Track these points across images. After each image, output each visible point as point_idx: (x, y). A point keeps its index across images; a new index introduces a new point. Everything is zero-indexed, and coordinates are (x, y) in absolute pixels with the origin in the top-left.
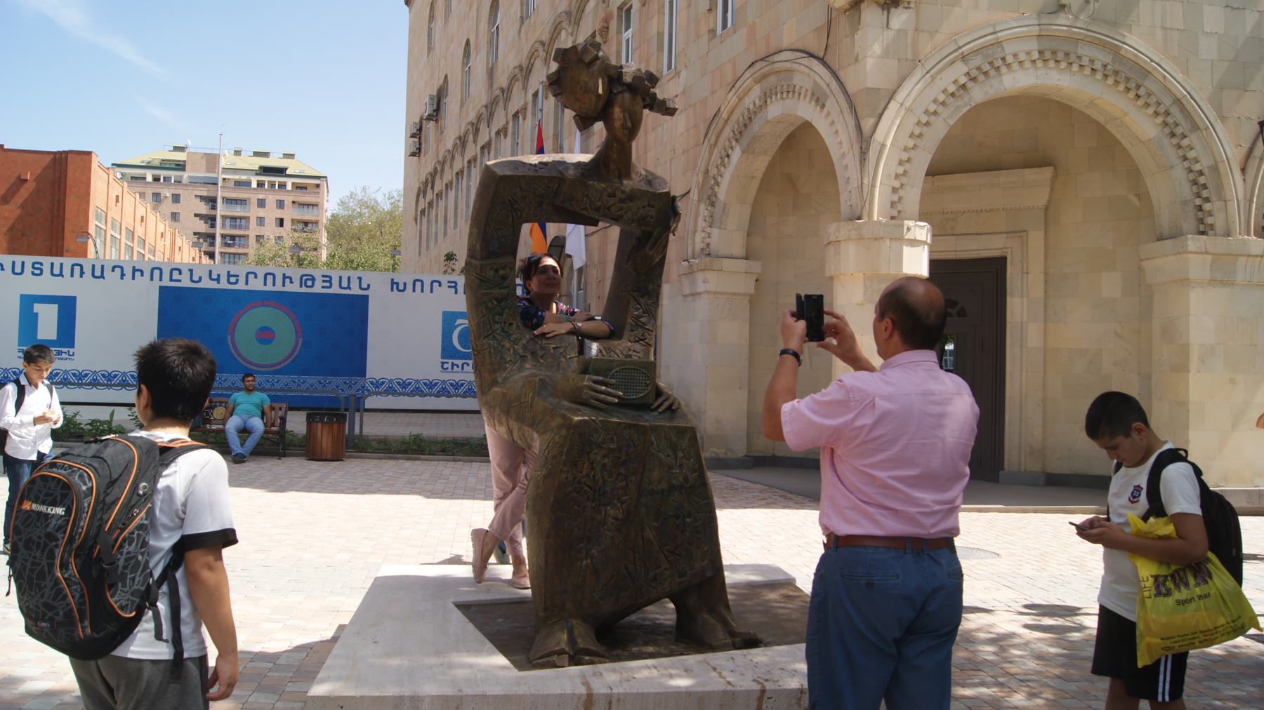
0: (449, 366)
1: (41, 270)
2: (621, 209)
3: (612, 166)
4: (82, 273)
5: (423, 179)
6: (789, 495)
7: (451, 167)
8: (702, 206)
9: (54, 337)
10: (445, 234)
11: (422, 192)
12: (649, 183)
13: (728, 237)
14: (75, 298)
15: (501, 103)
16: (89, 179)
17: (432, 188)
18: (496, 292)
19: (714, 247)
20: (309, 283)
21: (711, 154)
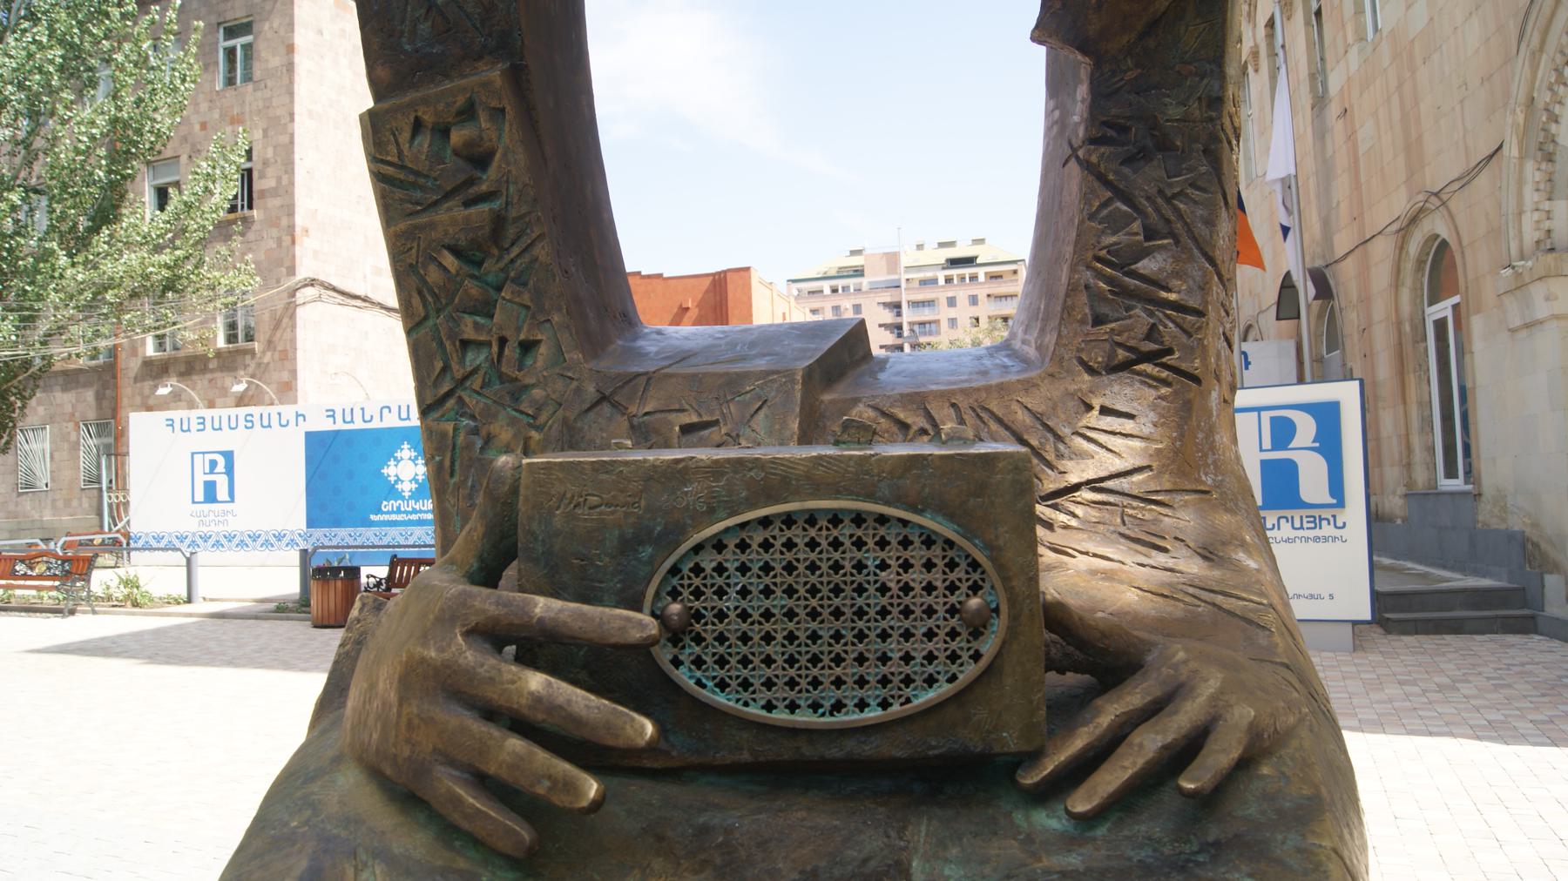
8: (1530, 166)
16: (750, 298)
18: (452, 218)
19: (1559, 237)
21: (1534, 67)
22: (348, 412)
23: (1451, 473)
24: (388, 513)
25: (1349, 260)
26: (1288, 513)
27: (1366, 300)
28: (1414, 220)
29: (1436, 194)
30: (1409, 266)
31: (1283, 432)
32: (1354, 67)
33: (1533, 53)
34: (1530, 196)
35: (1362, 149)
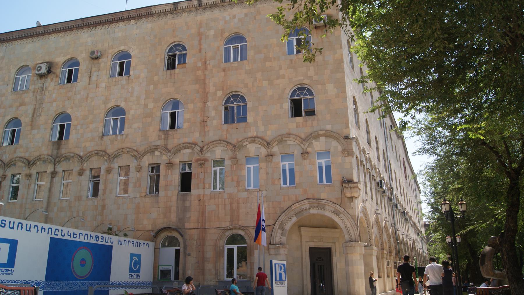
1: (5, 224)
4: (22, 228)
14: (17, 241)
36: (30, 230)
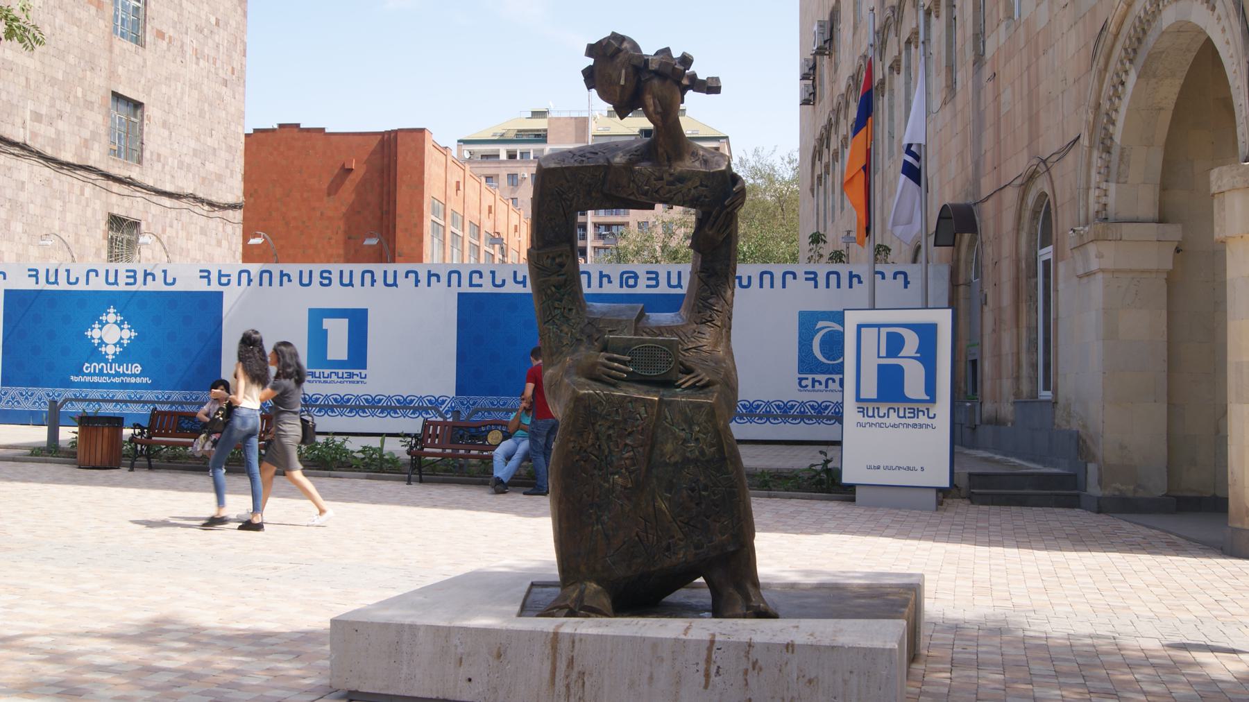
0: (809, 382)
1: (330, 279)
2: (670, 191)
3: (660, 150)
4: (373, 281)
5: (818, 135)
6: (1181, 541)
7: (846, 117)
8: (1095, 154)
9: (345, 357)
10: (842, 208)
11: (817, 154)
12: (706, 162)
13: (1135, 193)
15: (893, 27)
16: (422, 164)
17: (828, 147)
18: (554, 279)
20: (631, 282)
22: (52, 273)
23: (1047, 388)
24: (90, 374)
25: (990, 201)
26: (895, 405)
27: (998, 237)
28: (1032, 177)
29: (1044, 162)
30: (1027, 215)
31: (895, 344)
32: (1002, 41)
33: (1100, 72)
34: (1095, 178)
35: (1004, 110)
36: (351, 284)
